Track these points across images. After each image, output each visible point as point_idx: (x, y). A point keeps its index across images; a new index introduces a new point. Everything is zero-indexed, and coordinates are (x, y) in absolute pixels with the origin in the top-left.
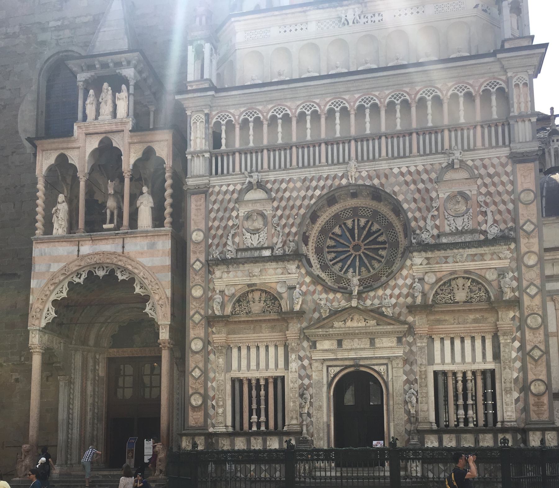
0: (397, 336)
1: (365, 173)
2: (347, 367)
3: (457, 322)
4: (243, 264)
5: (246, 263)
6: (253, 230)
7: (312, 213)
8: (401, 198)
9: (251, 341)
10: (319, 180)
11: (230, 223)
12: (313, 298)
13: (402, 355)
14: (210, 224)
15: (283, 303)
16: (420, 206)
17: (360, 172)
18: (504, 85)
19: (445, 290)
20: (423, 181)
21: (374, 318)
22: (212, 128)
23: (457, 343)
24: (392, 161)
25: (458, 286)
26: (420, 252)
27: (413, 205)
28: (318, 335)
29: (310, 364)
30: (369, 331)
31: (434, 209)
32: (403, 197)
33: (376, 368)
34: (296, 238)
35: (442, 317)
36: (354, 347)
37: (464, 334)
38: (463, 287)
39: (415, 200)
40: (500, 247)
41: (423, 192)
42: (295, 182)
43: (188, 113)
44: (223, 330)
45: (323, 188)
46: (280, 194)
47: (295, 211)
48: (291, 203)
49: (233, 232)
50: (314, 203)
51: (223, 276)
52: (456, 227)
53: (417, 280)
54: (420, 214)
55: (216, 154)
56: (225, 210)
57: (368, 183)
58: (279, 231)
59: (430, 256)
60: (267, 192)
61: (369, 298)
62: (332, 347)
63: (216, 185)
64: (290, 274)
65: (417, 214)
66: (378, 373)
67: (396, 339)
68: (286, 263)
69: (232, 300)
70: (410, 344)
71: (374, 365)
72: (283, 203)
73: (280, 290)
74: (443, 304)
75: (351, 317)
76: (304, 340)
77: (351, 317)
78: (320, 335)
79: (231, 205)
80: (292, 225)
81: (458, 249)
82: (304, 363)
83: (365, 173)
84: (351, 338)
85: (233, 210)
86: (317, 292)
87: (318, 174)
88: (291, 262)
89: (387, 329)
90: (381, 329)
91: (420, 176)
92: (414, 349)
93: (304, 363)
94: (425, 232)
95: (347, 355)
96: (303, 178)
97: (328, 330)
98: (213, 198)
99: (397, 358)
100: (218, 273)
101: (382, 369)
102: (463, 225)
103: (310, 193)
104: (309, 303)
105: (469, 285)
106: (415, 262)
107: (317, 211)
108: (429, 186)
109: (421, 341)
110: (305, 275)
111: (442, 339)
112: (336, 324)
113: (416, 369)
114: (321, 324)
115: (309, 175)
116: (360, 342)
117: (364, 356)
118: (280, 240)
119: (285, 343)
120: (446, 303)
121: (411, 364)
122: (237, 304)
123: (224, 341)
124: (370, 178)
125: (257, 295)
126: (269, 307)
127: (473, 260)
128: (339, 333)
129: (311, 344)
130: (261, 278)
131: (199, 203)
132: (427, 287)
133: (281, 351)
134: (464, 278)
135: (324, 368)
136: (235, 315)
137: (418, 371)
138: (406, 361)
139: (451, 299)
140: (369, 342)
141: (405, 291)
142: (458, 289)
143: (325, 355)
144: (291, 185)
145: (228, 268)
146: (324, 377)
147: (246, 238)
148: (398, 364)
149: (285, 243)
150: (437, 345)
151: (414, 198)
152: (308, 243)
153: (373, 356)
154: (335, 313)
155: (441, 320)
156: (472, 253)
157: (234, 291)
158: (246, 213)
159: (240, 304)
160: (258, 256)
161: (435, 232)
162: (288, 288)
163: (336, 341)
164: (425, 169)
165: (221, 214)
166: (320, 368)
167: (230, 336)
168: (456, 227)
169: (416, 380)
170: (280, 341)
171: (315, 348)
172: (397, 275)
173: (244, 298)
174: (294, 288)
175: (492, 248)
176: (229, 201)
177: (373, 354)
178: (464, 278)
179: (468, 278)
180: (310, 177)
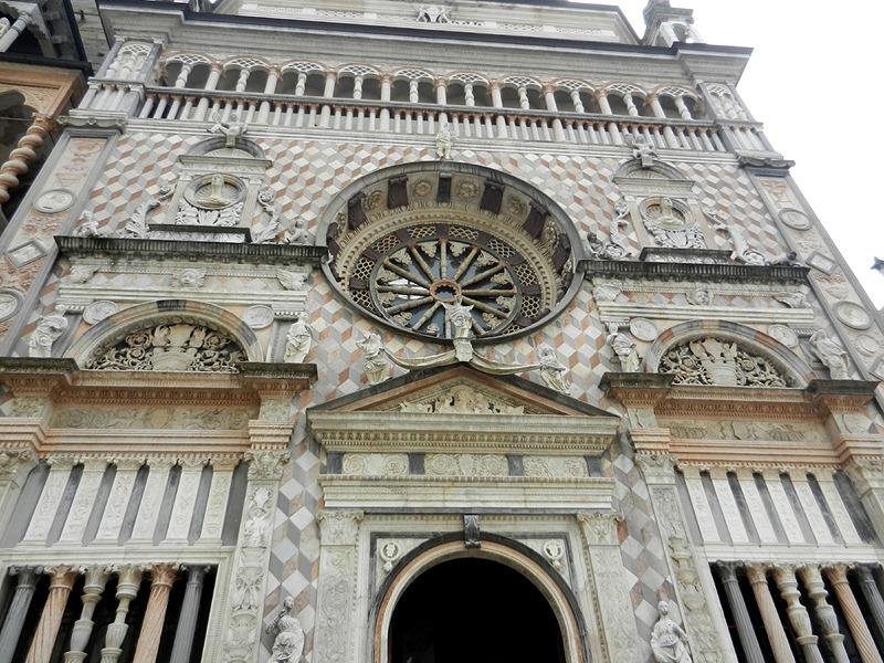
0: (588, 452)
2: (437, 540)
3: (730, 434)
5: (169, 256)
7: (355, 196)
9: (127, 449)
10: (375, 150)
11: (153, 190)
13: (609, 506)
14: (100, 185)
18: (691, 94)
19: (683, 359)
20: (589, 178)
21: (515, 401)
22: (161, 64)
23: (748, 487)
25: (708, 355)
26: (610, 276)
27: (575, 207)
28: (350, 432)
29: (317, 524)
30: (508, 429)
32: (554, 193)
33: (535, 545)
34: (313, 230)
35: (690, 422)
39: (578, 200)
42: (320, 147)
43: (119, 38)
44: (40, 408)
45: (383, 161)
46: (284, 161)
49: (153, 202)
55: (157, 94)
56: (148, 169)
58: (270, 214)
59: (631, 289)
60: (255, 154)
65: (587, 221)
66: (543, 563)
67: (583, 461)
68: (278, 267)
70: (624, 478)
71: (524, 536)
72: (291, 174)
73: (250, 323)
75: (451, 394)
76: (304, 449)
77: (451, 394)
78: (359, 432)
79: (164, 164)
80: (306, 208)
84: (451, 450)
85: (165, 171)
86: (355, 334)
89: (560, 426)
90: (545, 426)
92: (639, 489)
95: (441, 498)
98: (124, 149)
99: (596, 515)
100: (80, 269)
101: (553, 550)
103: (353, 166)
104: (329, 356)
106: (601, 295)
108: (602, 185)
110: (326, 298)
112: (406, 407)
113: (658, 549)
114: (366, 403)
116: (479, 463)
117: (493, 505)
121: (642, 538)
122: (113, 352)
123: (31, 437)
124: (479, 159)
125: (179, 336)
126: (211, 364)
129: (325, 464)
131: (85, 152)
133: (222, 482)
135: (361, 538)
137: (669, 560)
138: (622, 526)
139: (701, 380)
140: (506, 464)
141: (588, 351)
143: (369, 497)
144: (313, 151)
146: (359, 571)
148: (601, 535)
153: (522, 506)
154: (418, 376)
159: (123, 350)
161: (636, 253)
162: (275, 320)
163: (407, 457)
165: (132, 174)
166: (348, 538)
167: (55, 431)
169: (668, 587)
170: (225, 453)
171: (339, 469)
172: (561, 317)
174: (296, 320)
176: (164, 156)
177: (523, 498)
178: (718, 339)
179: (730, 342)
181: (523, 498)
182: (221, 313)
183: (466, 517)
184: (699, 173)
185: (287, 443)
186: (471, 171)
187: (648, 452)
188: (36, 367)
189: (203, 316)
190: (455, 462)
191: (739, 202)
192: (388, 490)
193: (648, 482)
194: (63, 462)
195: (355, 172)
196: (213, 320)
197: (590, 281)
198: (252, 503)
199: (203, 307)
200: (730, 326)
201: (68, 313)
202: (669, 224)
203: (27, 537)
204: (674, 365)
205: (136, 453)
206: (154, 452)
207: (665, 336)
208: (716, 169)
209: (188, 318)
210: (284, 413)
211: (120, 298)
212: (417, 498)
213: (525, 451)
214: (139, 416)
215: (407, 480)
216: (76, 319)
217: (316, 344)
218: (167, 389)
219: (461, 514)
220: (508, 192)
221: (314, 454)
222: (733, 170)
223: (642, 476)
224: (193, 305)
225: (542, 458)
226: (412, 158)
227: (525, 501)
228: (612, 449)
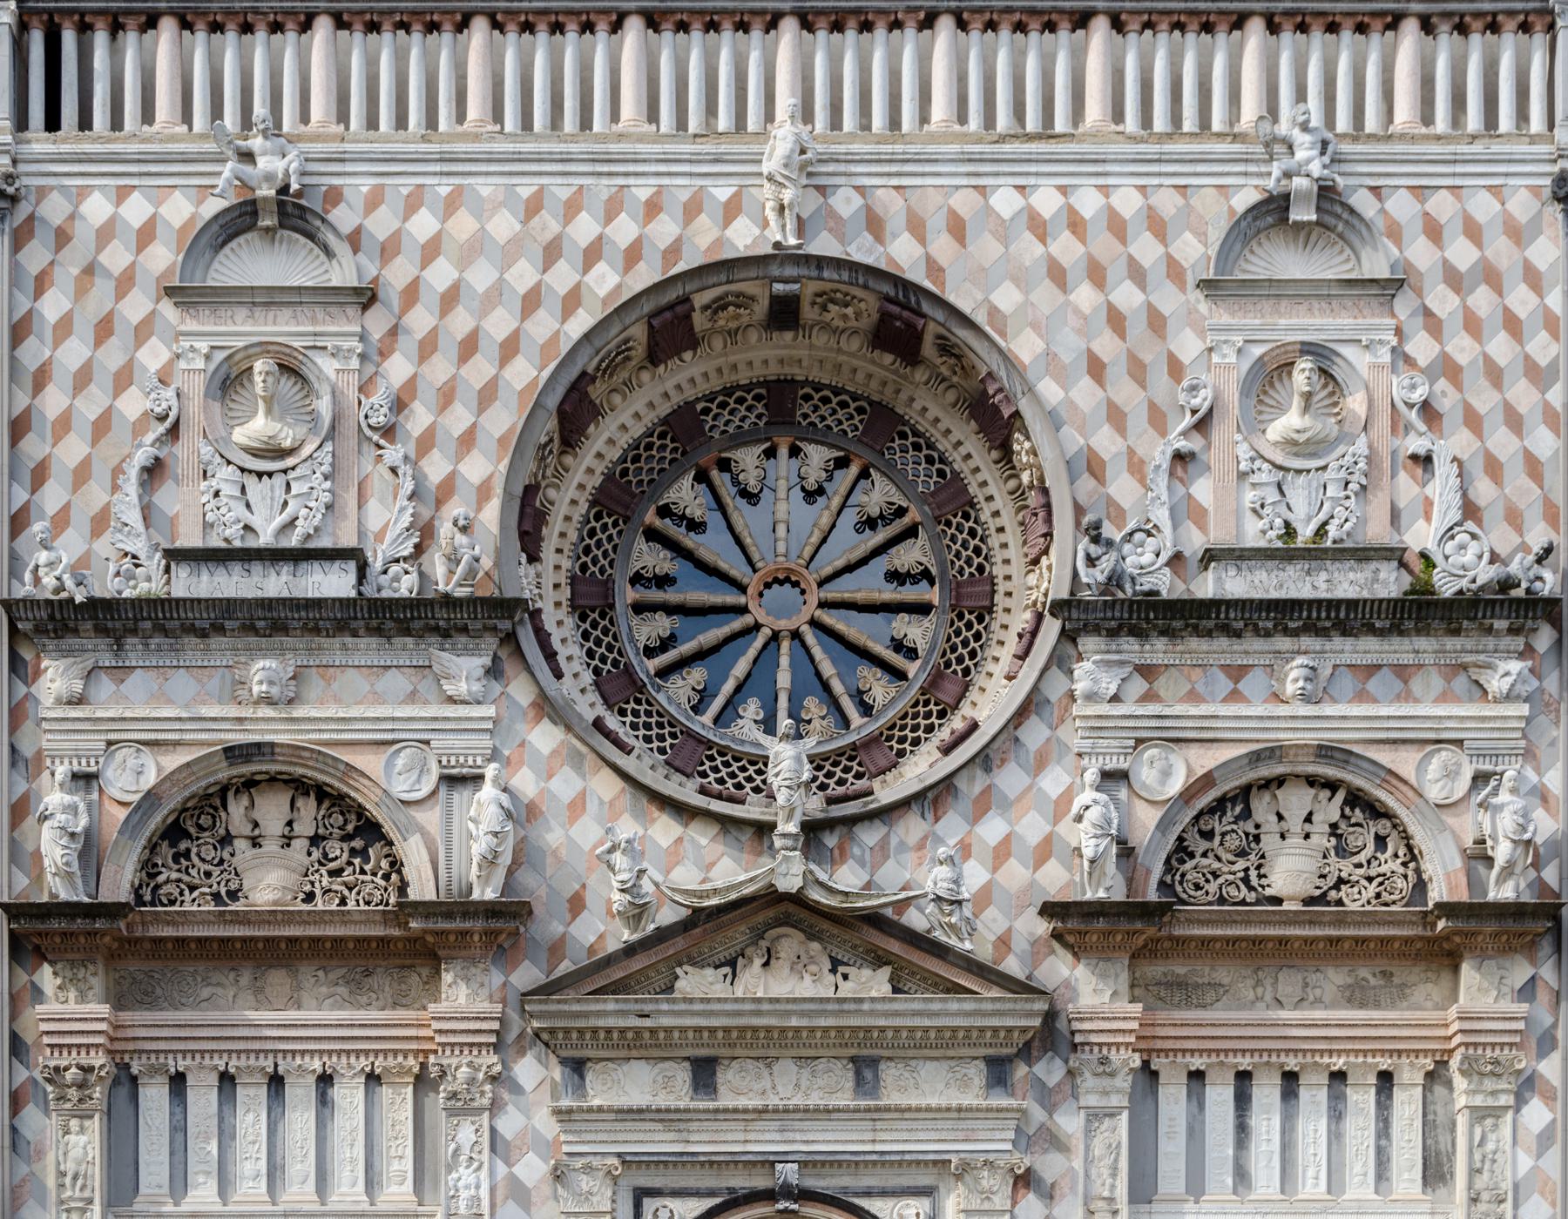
0: (991, 1051)
1: (848, 200)
4: (203, 634)
5: (220, 630)
6: (255, 453)
8: (1026, 347)
9: (241, 1046)
11: (132, 405)
12: (568, 836)
13: (1009, 1146)
15: (414, 855)
16: (1118, 400)
17: (821, 189)
19: (1223, 835)
20: (1137, 274)
21: (878, 959)
23: (1266, 1093)
24: (987, 148)
25: (1280, 817)
26: (1113, 633)
27: (1085, 393)
31: (1188, 420)
32: (1040, 345)
35: (1203, 971)
36: (773, 1101)
37: (1300, 1059)
38: (1307, 827)
39: (1096, 369)
40: (1490, 642)
41: (1137, 328)
45: (633, 255)
47: (480, 370)
48: (461, 322)
50: (587, 337)
51: (92, 691)
52: (1287, 524)
53: (1091, 775)
54: (1119, 440)
55: (50, 13)
57: (862, 251)
59: (1158, 659)
61: (856, 851)
62: (663, 1101)
63: (52, 188)
64: (451, 700)
67: (982, 1065)
69: (142, 822)
73: (401, 787)
74: (1210, 903)
75: (764, 944)
76: (522, 1052)
79: (136, 307)
80: (468, 440)
81: (1295, 633)
82: (518, 1170)
83: (848, 200)
85: (143, 331)
86: (592, 806)
87: (605, 181)
88: (462, 640)
91: (1123, 241)
93: (518, 1170)
94: (1139, 536)
95: (741, 1137)
96: (525, 192)
97: (648, 1008)
102: (1322, 517)
103: (562, 277)
105: (1335, 816)
107: (593, 379)
108: (1169, 300)
109: (1106, 1082)
110: (531, 714)
111: (1197, 1076)
115: (559, 180)
116: (806, 1073)
118: (406, 519)
119: (423, 1066)
120: (1222, 900)
121: (1049, 1195)
122: (166, 851)
127: (1362, 696)
128: (703, 1022)
130: (299, 712)
132: (1146, 819)
134: (1311, 781)
135: (619, 1199)
136: (153, 904)
140: (851, 1075)
142: (1283, 837)
144: (463, 225)
145: (120, 647)
147: (217, 494)
149: (425, 534)
150: (1173, 1097)
151: (1089, 350)
152: (538, 548)
155: (1197, 986)
156: (1357, 659)
157: (150, 779)
158: (220, 356)
160: (285, 594)
163: (687, 1064)
164: (1150, 208)
168: (1287, 524)
171: (580, 1089)
173: (205, 821)
174: (478, 779)
175: (1452, 643)
177: (869, 1136)
178: (1311, 781)
179: (1332, 786)
180: (564, 194)
181: (869, 1136)
182: (342, 767)
183: (779, 1167)
184: (1434, 231)
185: (494, 1045)
186: (845, 276)
187: (1096, 1049)
188: (73, 917)
189: (310, 773)
190: (766, 1072)
191: (1500, 347)
192: (659, 1126)
193: (1082, 1103)
194: (154, 1071)
195: (572, 302)
196: (328, 780)
197: (1074, 641)
198: (453, 1146)
199: (307, 754)
200: (1338, 755)
201: (75, 776)
202: (1295, 443)
203: (143, 1189)
204: (1203, 845)
205: (258, 1052)
206: (285, 1051)
207: (1193, 791)
208: (1483, 207)
209: (281, 773)
210: (482, 985)
211: (153, 736)
212: (705, 1137)
213: (885, 1053)
214: (246, 978)
215: (687, 1111)
216: (88, 790)
217: (522, 833)
218: (280, 938)
219: (768, 1163)
220: (932, 328)
221: (540, 1061)
222: (1521, 205)
223: (1076, 1097)
224: (285, 751)
225: (913, 1063)
226: (703, 243)
227: (874, 1141)
228: (1036, 1043)
